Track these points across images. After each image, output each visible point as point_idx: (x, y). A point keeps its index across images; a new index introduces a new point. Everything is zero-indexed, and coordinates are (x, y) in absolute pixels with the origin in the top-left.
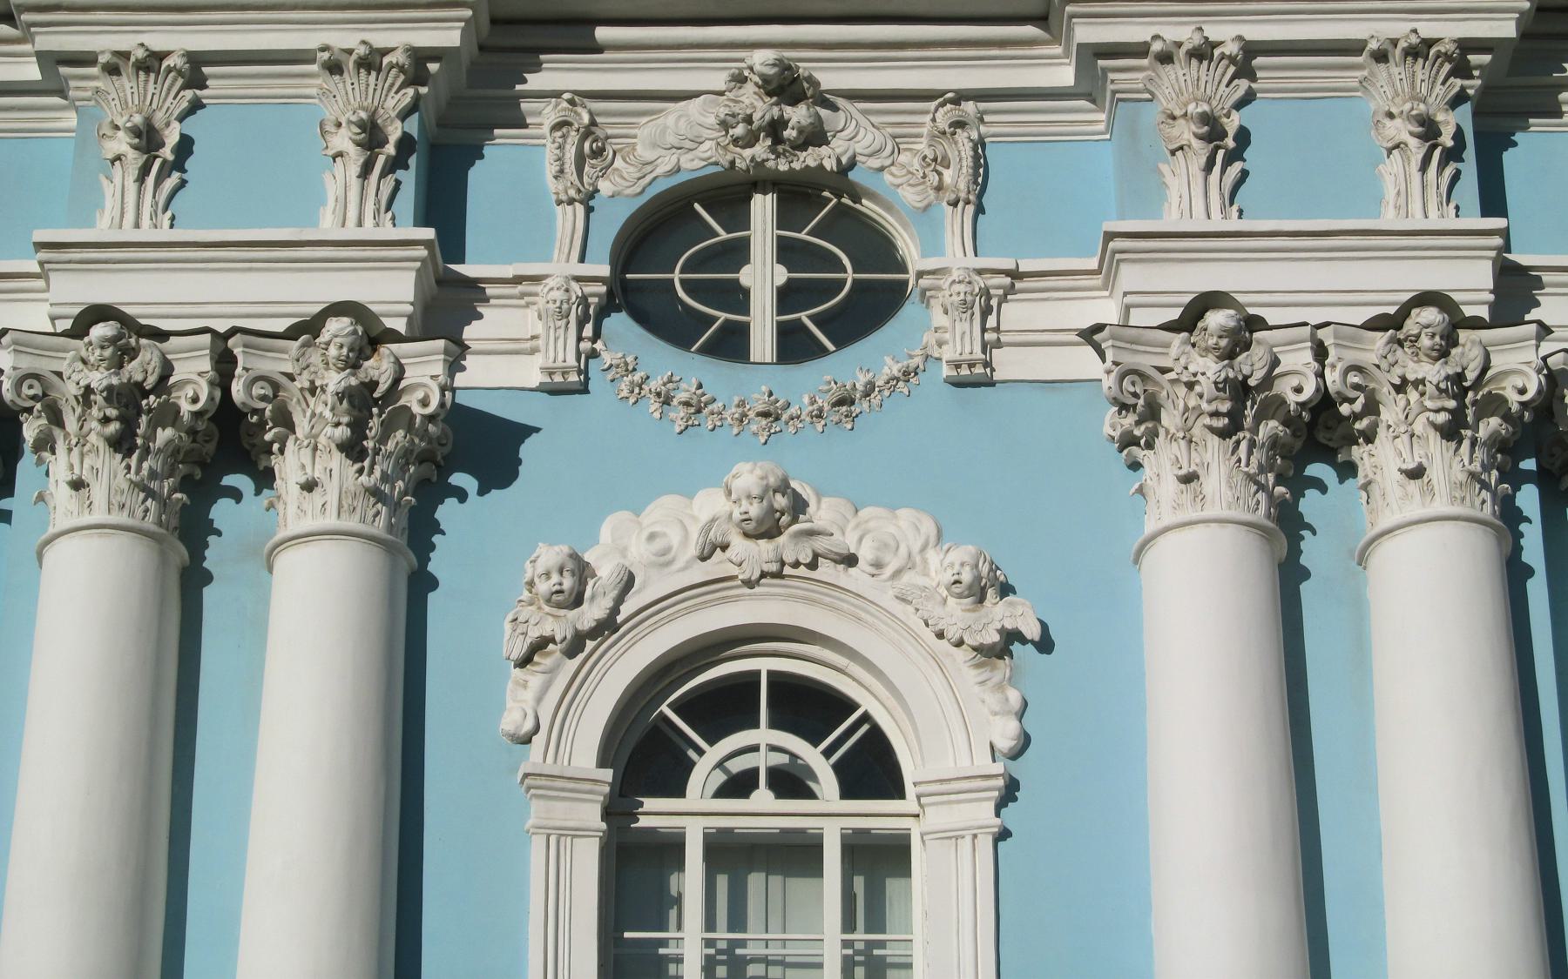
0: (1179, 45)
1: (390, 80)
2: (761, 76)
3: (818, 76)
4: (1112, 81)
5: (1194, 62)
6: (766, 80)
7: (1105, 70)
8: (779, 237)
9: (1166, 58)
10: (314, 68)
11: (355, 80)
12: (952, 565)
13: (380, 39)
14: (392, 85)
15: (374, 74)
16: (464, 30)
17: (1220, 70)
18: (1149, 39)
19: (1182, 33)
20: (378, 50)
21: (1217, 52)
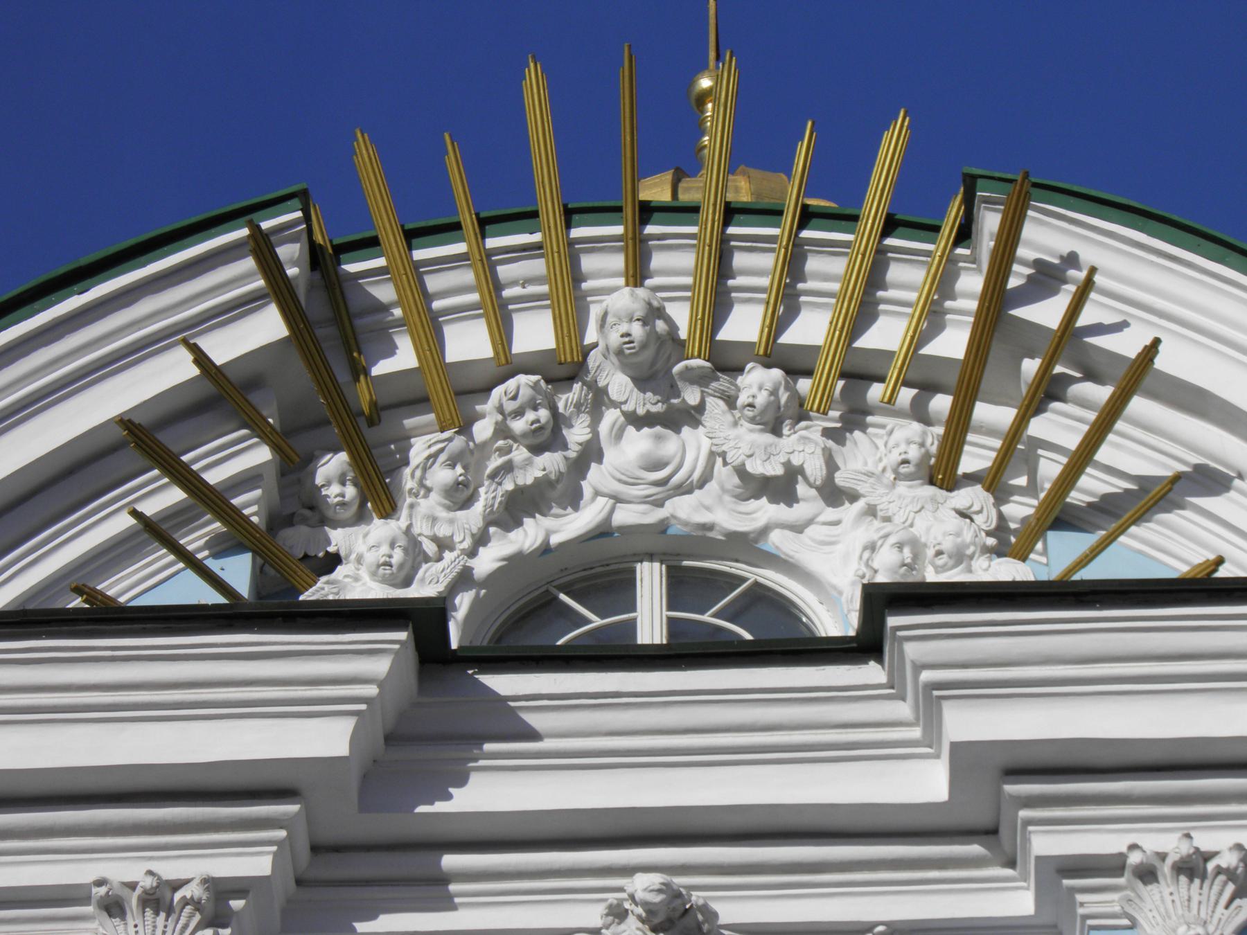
0: (1163, 857)
1: (183, 921)
2: (645, 904)
3: (715, 906)
4: (1082, 904)
5: (1183, 879)
6: (650, 910)
7: (1074, 890)
8: (670, 619)
9: (1147, 874)
10: (89, 909)
11: (139, 921)
12: (897, 445)
13: (170, 869)
14: (185, 927)
15: (163, 915)
16: (276, 855)
17: (1216, 888)
18: (1124, 849)
19: (1165, 842)
20: (168, 882)
21: (1211, 866)
